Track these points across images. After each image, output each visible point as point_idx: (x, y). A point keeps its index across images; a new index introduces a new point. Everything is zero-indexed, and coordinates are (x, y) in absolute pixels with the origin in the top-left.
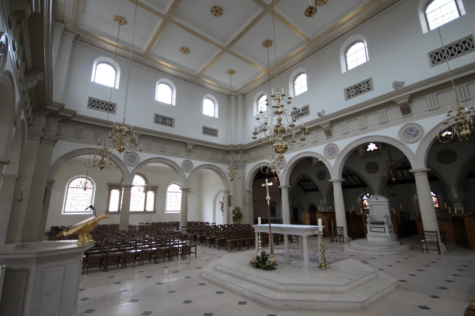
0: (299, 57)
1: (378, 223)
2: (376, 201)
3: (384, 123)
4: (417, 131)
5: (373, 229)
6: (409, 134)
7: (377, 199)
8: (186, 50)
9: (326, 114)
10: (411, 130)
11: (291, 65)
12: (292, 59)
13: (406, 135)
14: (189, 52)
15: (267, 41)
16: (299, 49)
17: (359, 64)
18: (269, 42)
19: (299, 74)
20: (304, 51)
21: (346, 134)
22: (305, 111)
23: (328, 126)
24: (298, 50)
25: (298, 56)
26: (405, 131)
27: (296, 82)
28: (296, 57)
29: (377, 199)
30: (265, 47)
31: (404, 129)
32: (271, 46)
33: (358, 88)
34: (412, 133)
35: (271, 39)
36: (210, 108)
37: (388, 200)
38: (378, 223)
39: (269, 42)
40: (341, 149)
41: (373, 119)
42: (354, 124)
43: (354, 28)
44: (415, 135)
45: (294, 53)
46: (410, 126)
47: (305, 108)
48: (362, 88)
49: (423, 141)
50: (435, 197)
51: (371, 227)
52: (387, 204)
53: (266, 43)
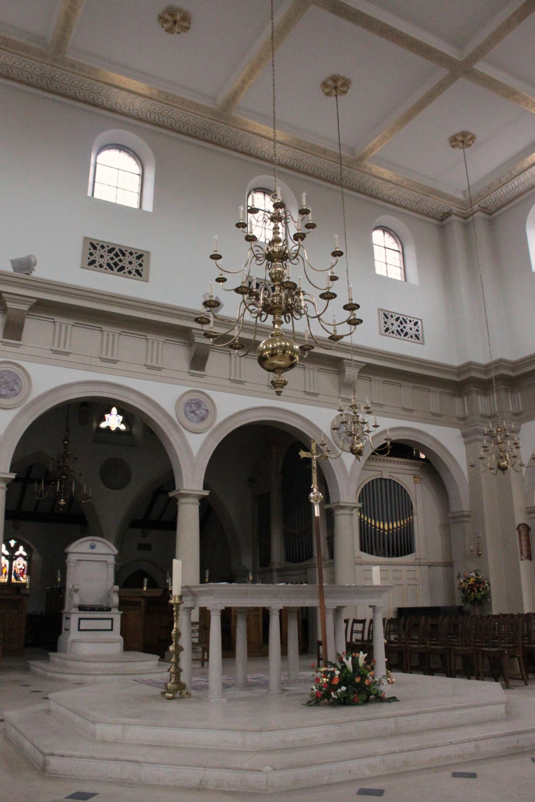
1: (92, 609)
2: (91, 551)
3: (154, 369)
4: (207, 411)
5: (84, 625)
6: (193, 412)
7: (93, 547)
9: (38, 273)
10: (198, 404)
13: (189, 414)
17: (119, 202)
21: (60, 354)
23: (26, 308)
26: (188, 404)
29: (93, 547)
31: (186, 399)
33: (117, 255)
34: (198, 412)
37: (116, 552)
38: (92, 609)
40: (37, 390)
41: (131, 346)
42: (86, 338)
43: (140, 119)
44: (203, 419)
46: (197, 396)
48: (125, 263)
49: (211, 435)
50: (25, 558)
51: (80, 619)
52: (111, 560)
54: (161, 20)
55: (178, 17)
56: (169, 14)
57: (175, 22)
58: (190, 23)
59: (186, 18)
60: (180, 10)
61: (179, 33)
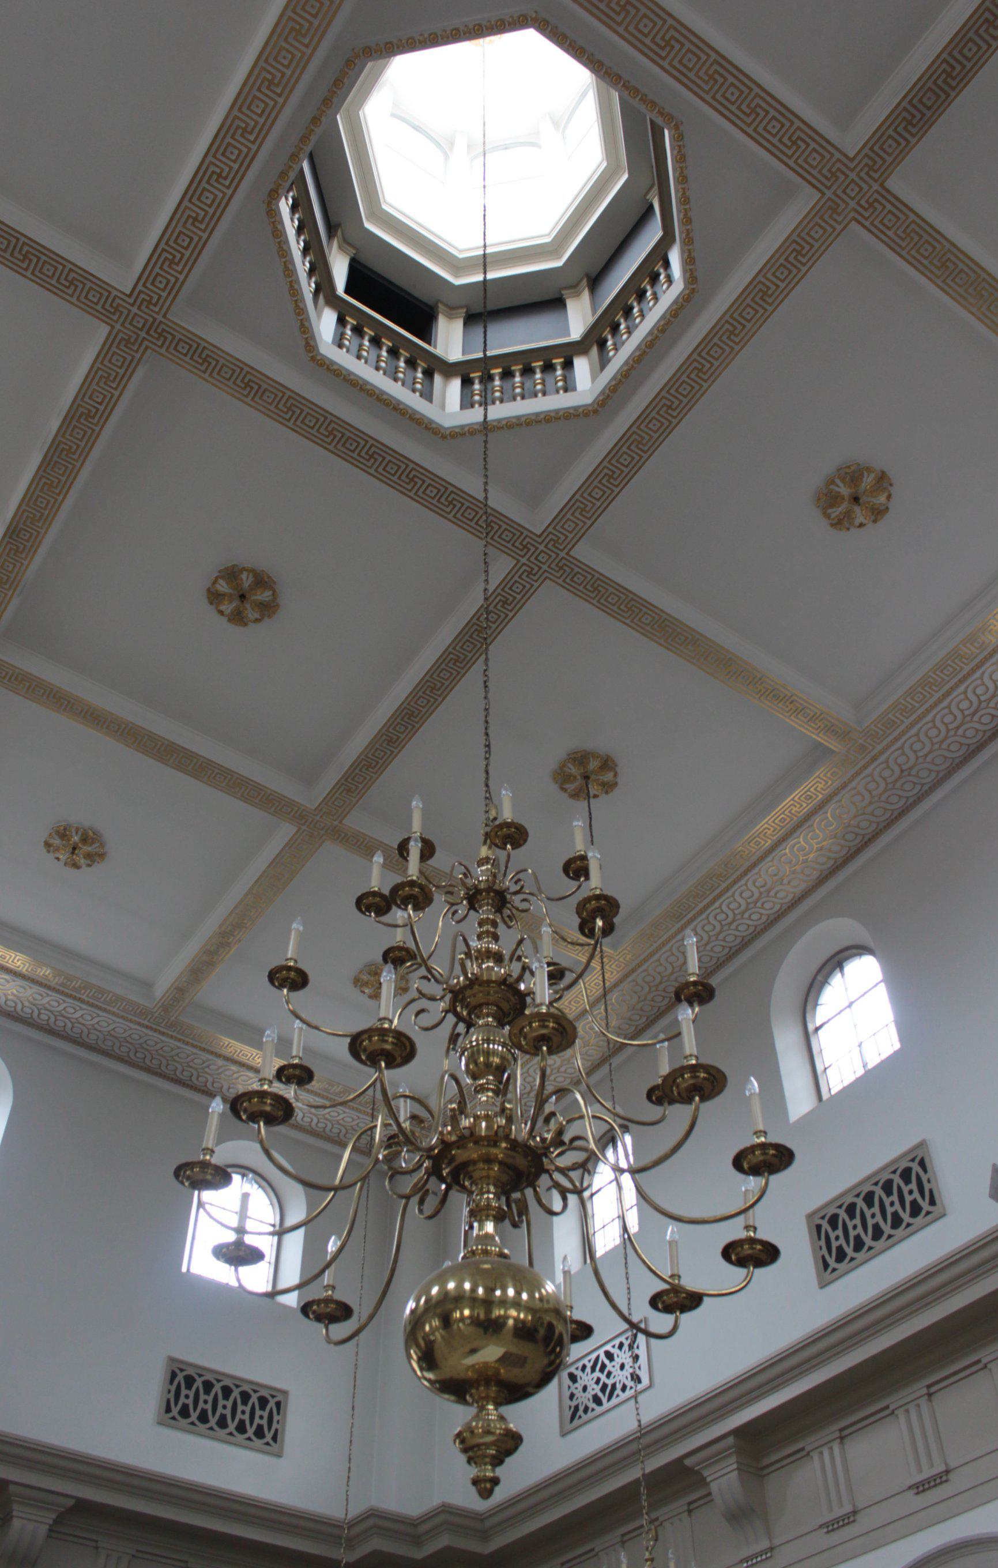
0: (812, 846)
8: (85, 840)
11: (771, 907)
12: (768, 868)
14: (102, 856)
15: (580, 758)
16: (796, 794)
18: (593, 765)
19: (836, 962)
20: (830, 810)
22: (903, 1194)
24: (794, 803)
25: (801, 840)
27: (821, 1014)
28: (787, 849)
30: (575, 795)
32: (608, 787)
35: (601, 743)
36: (240, 1233)
39: (593, 765)
45: (769, 825)
47: (906, 1174)
53: (573, 770)
54: (846, 524)
55: (845, 491)
56: (831, 506)
57: (856, 499)
58: (869, 470)
59: (852, 474)
60: (831, 482)
61: (889, 497)
